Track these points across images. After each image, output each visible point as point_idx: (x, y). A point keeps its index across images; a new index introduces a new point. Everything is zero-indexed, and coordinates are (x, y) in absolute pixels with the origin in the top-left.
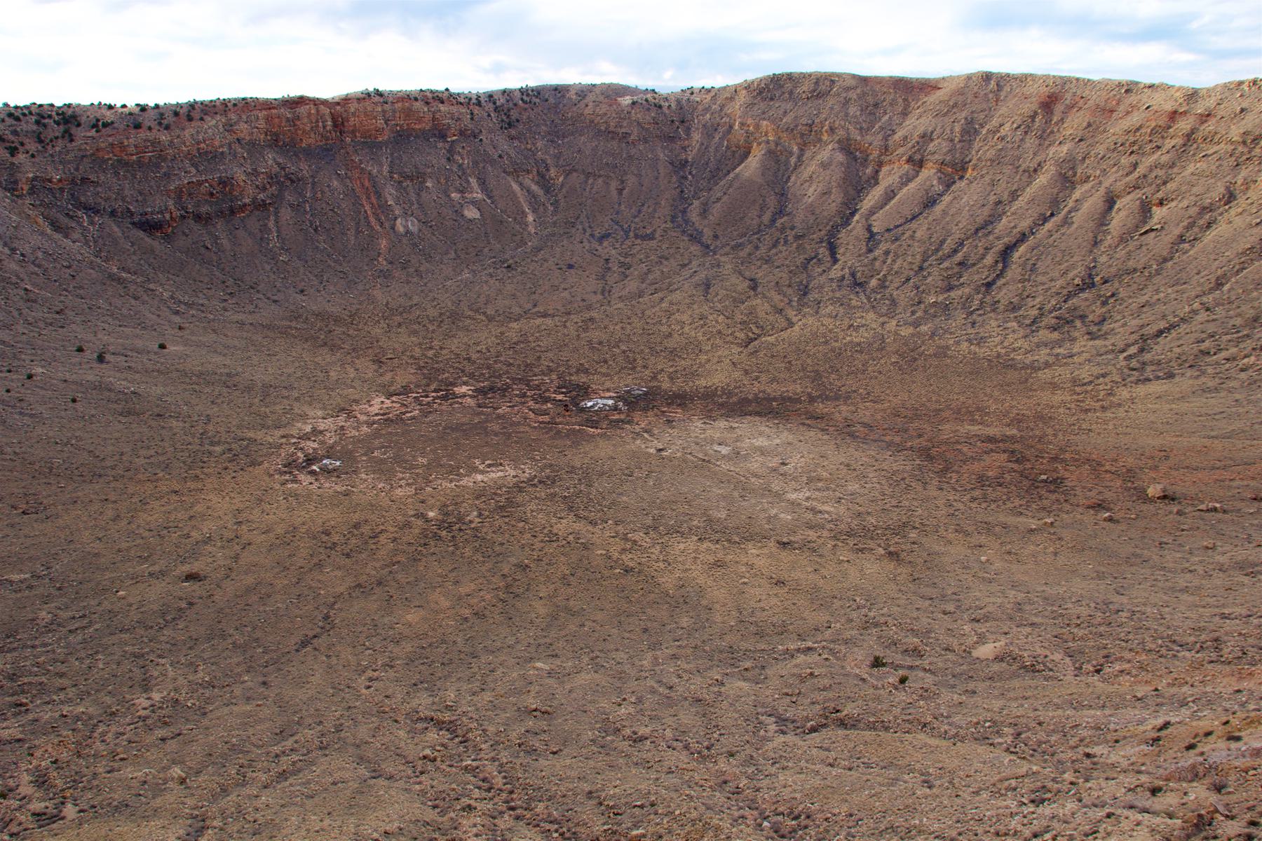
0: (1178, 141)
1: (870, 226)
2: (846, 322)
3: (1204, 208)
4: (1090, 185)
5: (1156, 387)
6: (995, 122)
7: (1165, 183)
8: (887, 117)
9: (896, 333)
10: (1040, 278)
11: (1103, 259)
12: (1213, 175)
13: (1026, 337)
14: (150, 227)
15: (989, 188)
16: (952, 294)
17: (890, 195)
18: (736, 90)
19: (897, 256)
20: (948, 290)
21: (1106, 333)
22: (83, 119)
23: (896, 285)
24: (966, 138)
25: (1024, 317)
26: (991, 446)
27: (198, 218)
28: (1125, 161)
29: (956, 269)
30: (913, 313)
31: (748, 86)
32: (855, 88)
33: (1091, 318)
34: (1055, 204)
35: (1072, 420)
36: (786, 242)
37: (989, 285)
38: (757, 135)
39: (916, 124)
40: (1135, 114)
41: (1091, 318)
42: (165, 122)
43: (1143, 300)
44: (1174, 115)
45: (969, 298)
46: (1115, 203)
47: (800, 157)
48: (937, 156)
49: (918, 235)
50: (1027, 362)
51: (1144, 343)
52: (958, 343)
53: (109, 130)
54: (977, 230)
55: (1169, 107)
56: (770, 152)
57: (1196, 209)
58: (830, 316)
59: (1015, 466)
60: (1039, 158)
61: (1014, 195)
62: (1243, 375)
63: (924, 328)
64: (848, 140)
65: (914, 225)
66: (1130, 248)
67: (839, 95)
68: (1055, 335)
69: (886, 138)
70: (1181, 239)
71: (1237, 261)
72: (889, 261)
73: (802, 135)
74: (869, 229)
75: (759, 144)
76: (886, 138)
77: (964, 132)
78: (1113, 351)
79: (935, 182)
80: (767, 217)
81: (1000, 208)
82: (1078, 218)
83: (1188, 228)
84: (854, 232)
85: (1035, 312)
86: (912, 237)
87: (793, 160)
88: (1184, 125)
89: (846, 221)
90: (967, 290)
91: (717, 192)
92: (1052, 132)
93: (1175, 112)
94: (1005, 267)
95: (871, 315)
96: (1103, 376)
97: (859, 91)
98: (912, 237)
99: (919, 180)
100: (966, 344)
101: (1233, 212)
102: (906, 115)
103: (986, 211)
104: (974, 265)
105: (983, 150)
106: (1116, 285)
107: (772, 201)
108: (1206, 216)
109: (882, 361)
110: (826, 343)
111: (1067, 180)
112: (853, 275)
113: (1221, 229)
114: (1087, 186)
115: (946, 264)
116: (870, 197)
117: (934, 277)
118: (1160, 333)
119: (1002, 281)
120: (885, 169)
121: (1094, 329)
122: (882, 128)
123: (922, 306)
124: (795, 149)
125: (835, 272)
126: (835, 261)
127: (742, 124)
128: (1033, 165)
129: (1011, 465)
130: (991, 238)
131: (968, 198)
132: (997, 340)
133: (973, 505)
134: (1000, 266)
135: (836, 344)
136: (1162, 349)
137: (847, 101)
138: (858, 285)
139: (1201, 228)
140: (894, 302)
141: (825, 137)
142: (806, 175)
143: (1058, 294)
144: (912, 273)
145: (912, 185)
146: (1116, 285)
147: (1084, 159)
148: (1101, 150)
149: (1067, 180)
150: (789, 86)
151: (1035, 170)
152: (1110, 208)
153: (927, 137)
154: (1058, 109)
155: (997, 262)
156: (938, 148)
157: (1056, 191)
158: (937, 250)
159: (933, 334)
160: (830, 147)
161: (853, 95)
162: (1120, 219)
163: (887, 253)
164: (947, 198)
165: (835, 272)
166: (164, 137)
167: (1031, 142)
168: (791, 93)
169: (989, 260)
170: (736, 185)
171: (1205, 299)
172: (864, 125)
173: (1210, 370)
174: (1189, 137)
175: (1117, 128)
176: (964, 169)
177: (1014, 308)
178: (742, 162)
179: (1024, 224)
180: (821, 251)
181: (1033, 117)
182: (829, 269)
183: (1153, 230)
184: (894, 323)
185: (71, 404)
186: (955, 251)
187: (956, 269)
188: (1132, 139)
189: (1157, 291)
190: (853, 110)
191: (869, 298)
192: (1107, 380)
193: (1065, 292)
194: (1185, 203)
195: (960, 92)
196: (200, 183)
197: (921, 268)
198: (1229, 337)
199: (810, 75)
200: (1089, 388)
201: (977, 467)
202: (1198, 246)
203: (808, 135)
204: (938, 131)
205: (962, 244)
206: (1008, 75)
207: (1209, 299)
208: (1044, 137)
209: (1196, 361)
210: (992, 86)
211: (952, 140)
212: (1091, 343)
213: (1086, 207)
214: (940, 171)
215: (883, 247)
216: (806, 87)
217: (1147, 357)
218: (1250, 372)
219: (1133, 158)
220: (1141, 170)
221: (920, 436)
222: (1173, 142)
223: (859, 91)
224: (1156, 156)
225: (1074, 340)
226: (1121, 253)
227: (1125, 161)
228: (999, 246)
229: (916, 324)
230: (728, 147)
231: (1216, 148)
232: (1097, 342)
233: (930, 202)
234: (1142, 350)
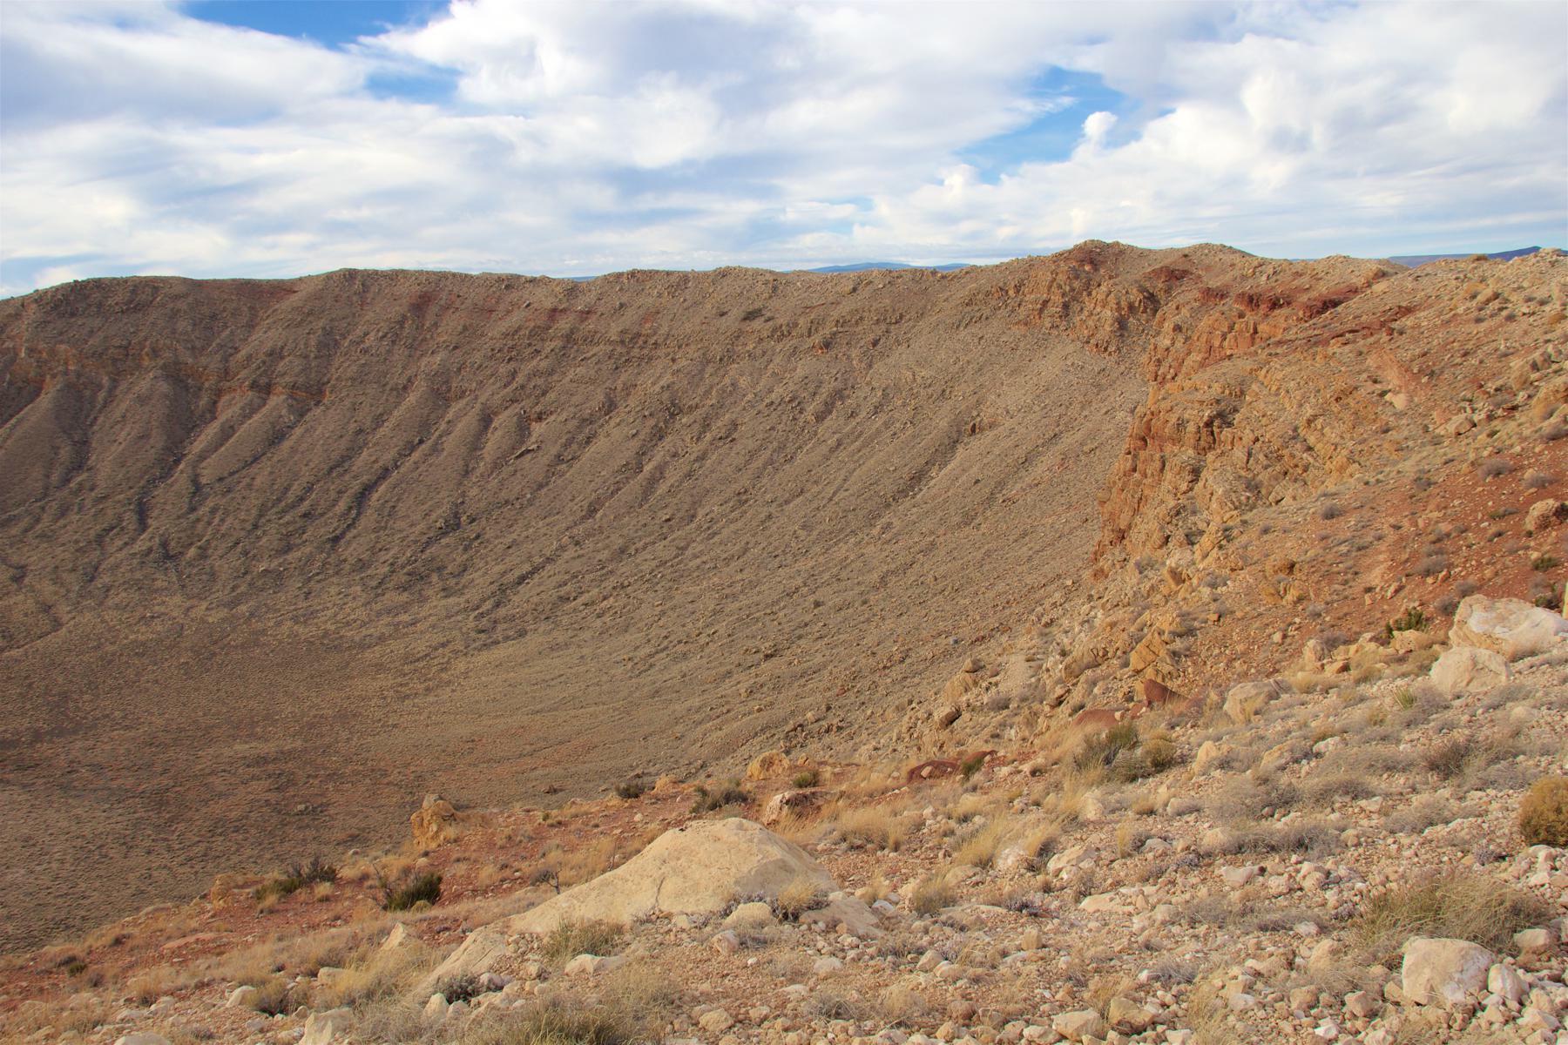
0: (558, 343)
1: (197, 475)
2: (137, 615)
3: (584, 420)
4: (464, 401)
5: (499, 653)
6: (359, 332)
7: (544, 394)
8: (227, 332)
9: (203, 621)
10: (400, 524)
11: (474, 492)
12: (592, 381)
13: (364, 605)
15: (348, 415)
16: (289, 557)
17: (227, 432)
18: (22, 304)
19: (227, 513)
20: (286, 552)
21: (464, 587)
23: (220, 552)
24: (325, 352)
25: (371, 577)
26: (256, 770)
28: (504, 369)
29: (300, 523)
30: (234, 589)
31: (39, 298)
32: (186, 296)
33: (450, 569)
34: (425, 426)
35: (379, 714)
36: (80, 509)
37: (336, 540)
38: (54, 364)
39: (265, 337)
40: (516, 312)
41: (450, 569)
43: (509, 540)
44: (554, 313)
45: (310, 559)
46: (491, 421)
47: (111, 391)
48: (287, 379)
49: (258, 482)
50: (357, 639)
51: (502, 593)
52: (279, 624)
54: (331, 469)
55: (548, 304)
56: (69, 386)
57: (575, 422)
58: (117, 607)
59: (273, 797)
60: (409, 373)
61: (379, 421)
62: (599, 622)
63: (243, 608)
64: (177, 363)
65: (254, 470)
66: (503, 475)
67: (163, 306)
68: (405, 597)
69: (226, 359)
70: (559, 459)
71: (612, 480)
72: (216, 521)
73: (115, 361)
74: (195, 481)
75: (54, 376)
76: (226, 359)
77: (321, 345)
78: (465, 609)
79: (284, 412)
81: (361, 437)
82: (450, 443)
83: (567, 445)
84: (176, 487)
85: (386, 569)
86: (249, 486)
87: (102, 395)
88: (564, 324)
89: (167, 472)
90: (308, 550)
92: (425, 340)
93: (554, 310)
94: (359, 514)
95: (178, 599)
96: (443, 645)
97: (190, 299)
98: (249, 486)
99: (264, 410)
100: (289, 623)
101: (612, 423)
102: (253, 327)
104: (322, 515)
105: (343, 367)
106: (484, 521)
107: (65, 453)
108: (585, 429)
109: (166, 664)
110: (98, 647)
111: (441, 395)
112: (164, 545)
113: (600, 445)
114: (463, 402)
115: (287, 518)
116: (203, 437)
117: (270, 538)
118: (522, 579)
119: (354, 532)
120: (225, 398)
121: (452, 582)
122: (221, 346)
123: (248, 577)
124: (105, 381)
125: (140, 545)
126: (143, 525)
127: (31, 351)
128: (402, 381)
129: (269, 796)
130: (347, 477)
131: (324, 427)
132: (329, 613)
133: (181, 870)
134: (354, 512)
135: (110, 648)
136: (522, 599)
137: (175, 314)
138: (167, 555)
139: (580, 444)
140: (213, 576)
141: (146, 363)
142: (118, 414)
143: (415, 542)
144: (243, 533)
145: (256, 417)
146: (484, 521)
147: (459, 370)
148: (477, 357)
149: (441, 395)
150: (97, 296)
151: (405, 388)
152: (486, 427)
153: (276, 355)
154: (433, 309)
155: (350, 508)
156: (289, 368)
157: (426, 411)
158: (279, 500)
159: (252, 615)
160: (151, 375)
161: (182, 305)
162: (495, 441)
163: (214, 511)
164: (298, 431)
165: (140, 545)
167: (400, 353)
168: (100, 305)
169: (342, 506)
170: (18, 432)
171: (575, 531)
172: (198, 344)
173: (565, 620)
174: (569, 338)
175: (497, 329)
176: (321, 393)
177: (362, 565)
178: (32, 401)
179: (388, 457)
180: (127, 516)
181: (401, 323)
182: (134, 540)
183: (528, 451)
184: (204, 605)
186: (302, 499)
187: (300, 523)
188: (510, 343)
189: (527, 527)
190: (183, 325)
191: (180, 574)
192: (447, 650)
193: (424, 539)
194: (565, 415)
195: (318, 296)
197: (256, 527)
198: (591, 576)
199: (126, 281)
200: (421, 664)
201: (217, 808)
202: (577, 465)
203: (123, 361)
204: (290, 345)
205: (310, 489)
206: (376, 272)
207: (579, 530)
208: (416, 348)
209: (548, 613)
210: (354, 287)
211: (306, 357)
212: (444, 602)
214: (291, 396)
215: (210, 503)
216: (121, 296)
217: (502, 612)
218: (607, 618)
219: (513, 365)
220: (520, 379)
221: (165, 771)
222: (553, 345)
223: (190, 299)
224: (534, 362)
225: (423, 600)
226: (494, 483)
227: (504, 369)
228: (356, 486)
229: (233, 604)
230: (11, 383)
231: (596, 350)
232: (451, 600)
233: (277, 437)
234: (498, 605)
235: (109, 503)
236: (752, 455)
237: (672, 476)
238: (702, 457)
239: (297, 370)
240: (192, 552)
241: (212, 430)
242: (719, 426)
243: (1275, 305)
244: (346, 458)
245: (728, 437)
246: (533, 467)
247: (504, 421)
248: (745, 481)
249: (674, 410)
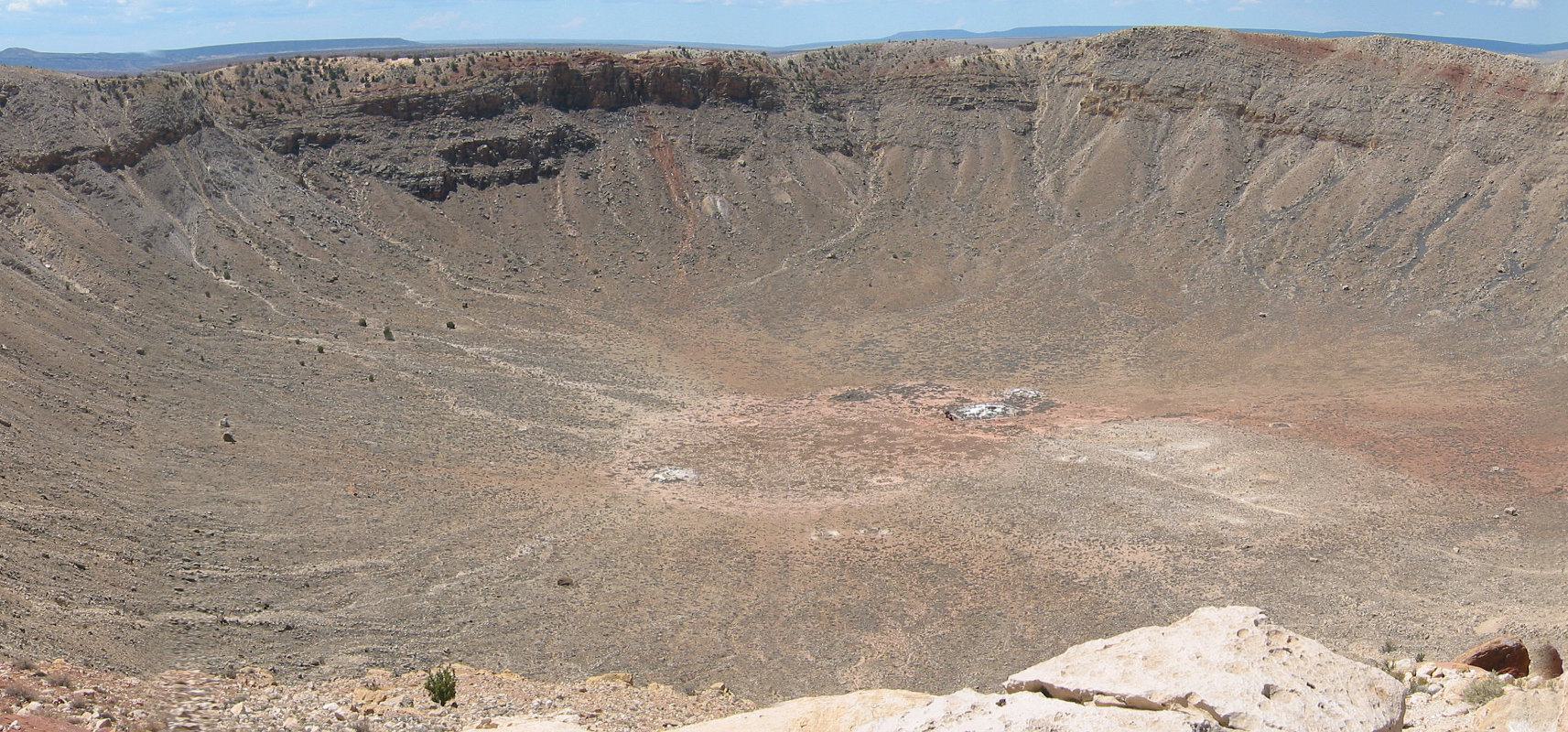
14: (424, 193)
22: (350, 73)
27: (470, 181)
42: (441, 77)
53: (380, 85)
54: (1386, 211)
61: (1426, 172)
67: (1212, 53)
75: (1121, 109)
80: (1135, 195)
107: (1139, 174)
130: (1402, 217)
161: (1233, 54)
166: (440, 89)
185: (369, 383)
196: (478, 144)
228: (1414, 228)
235: (1189, 217)
239: (1344, 120)
240: (1273, 266)
241: (1268, 166)
244: (1401, 202)
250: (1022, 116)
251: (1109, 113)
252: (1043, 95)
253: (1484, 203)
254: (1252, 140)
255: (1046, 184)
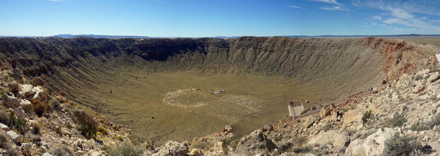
17: (262, 56)
61: (281, 55)
82: (291, 59)
91: (234, 56)
103: (277, 58)
107: (243, 57)
108: (309, 57)
113: (311, 60)
131: (274, 56)
137: (254, 41)
145: (265, 54)
162: (296, 59)
179: (283, 60)
213: (292, 57)
233: (268, 56)
236: (331, 61)
237: (321, 64)
238: (325, 61)
241: (260, 55)
242: (326, 58)
243: (393, 44)
244: (278, 60)
245: (328, 59)
246: (302, 62)
247: (297, 56)
248: (331, 64)
249: (320, 56)
250: (228, 49)
251: (239, 48)
252: (230, 45)
253: (289, 59)
254: (258, 52)
255: (230, 58)
